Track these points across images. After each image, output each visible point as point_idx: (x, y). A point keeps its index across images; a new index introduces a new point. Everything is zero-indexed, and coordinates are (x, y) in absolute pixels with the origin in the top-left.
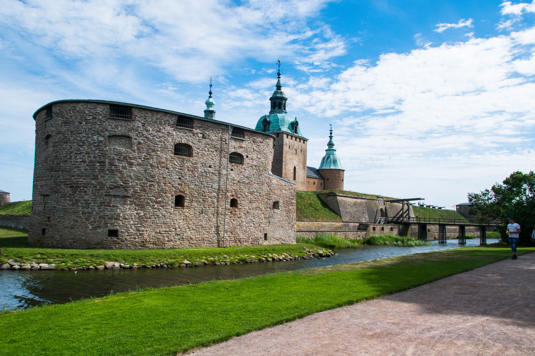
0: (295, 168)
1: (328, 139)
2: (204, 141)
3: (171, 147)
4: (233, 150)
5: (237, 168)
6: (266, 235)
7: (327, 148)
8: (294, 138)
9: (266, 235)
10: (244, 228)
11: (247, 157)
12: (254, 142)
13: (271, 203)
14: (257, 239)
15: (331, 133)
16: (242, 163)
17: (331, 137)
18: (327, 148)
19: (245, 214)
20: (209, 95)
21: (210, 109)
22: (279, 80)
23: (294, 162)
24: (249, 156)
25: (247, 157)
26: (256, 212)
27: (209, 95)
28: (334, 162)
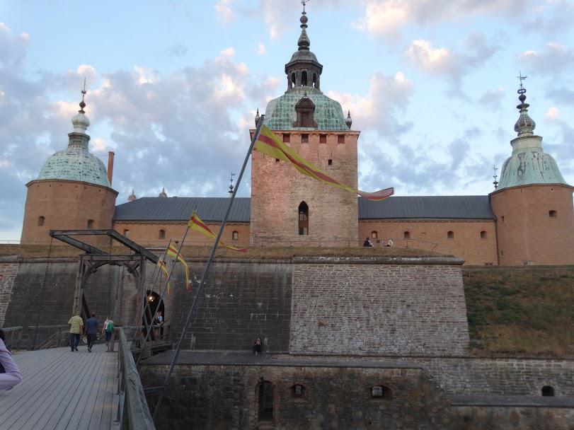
0: (303, 208)
1: (516, 116)
7: (515, 135)
8: (295, 139)
15: (522, 98)
17: (523, 107)
18: (515, 135)
20: (80, 109)
21: (79, 131)
22: (304, 34)
23: (301, 193)
27: (80, 109)
28: (520, 168)
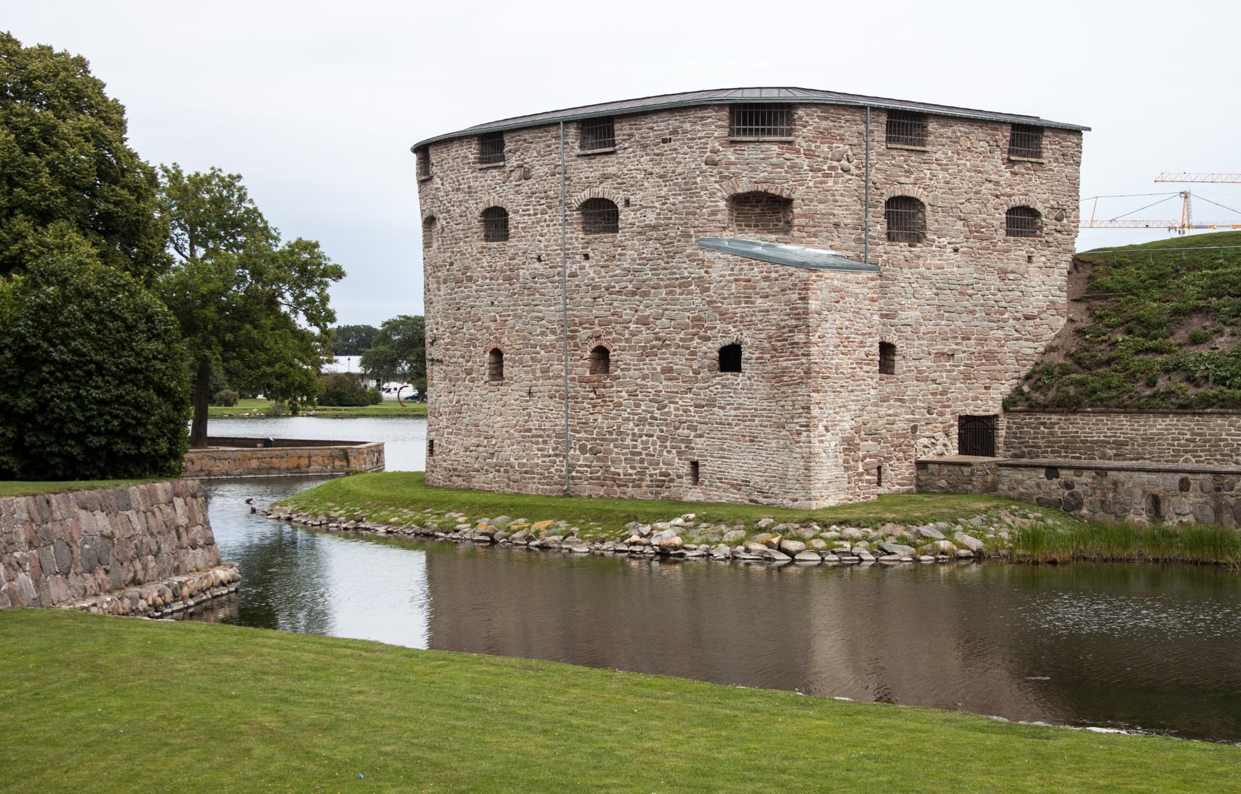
2: (526, 187)
3: (477, 225)
4: (585, 195)
5: (603, 244)
6: (695, 465)
9: (695, 465)
10: (628, 441)
11: (627, 203)
12: (645, 147)
13: (712, 349)
14: (664, 481)
16: (615, 229)
19: (632, 394)
24: (632, 199)
25: (627, 203)
26: (664, 385)
